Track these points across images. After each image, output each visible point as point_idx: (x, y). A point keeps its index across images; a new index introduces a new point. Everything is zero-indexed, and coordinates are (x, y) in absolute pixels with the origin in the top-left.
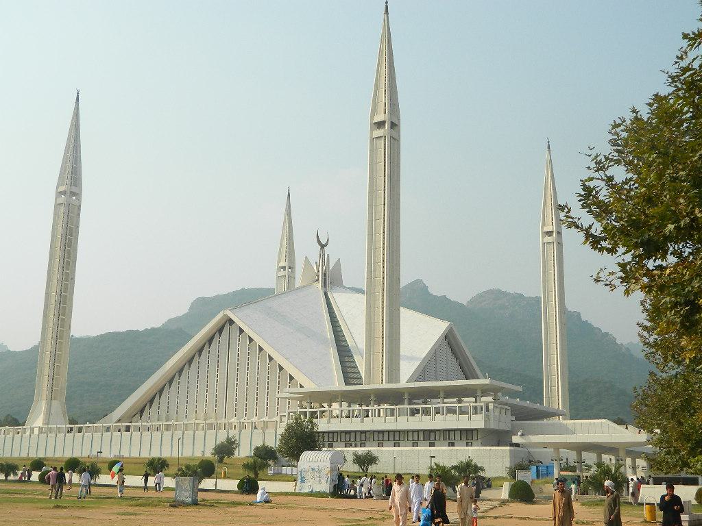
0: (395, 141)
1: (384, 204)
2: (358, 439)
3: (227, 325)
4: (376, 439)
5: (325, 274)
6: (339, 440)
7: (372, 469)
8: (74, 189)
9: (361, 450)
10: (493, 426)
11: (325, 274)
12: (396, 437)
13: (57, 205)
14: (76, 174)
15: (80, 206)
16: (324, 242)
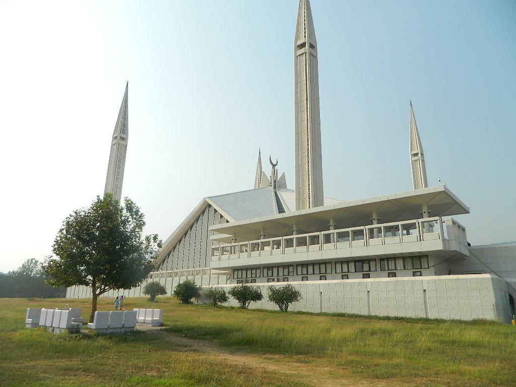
0: (313, 57)
1: (307, 100)
2: (281, 274)
3: (207, 210)
4: (300, 273)
5: (275, 181)
6: (262, 276)
7: (292, 307)
8: (123, 136)
9: (279, 285)
10: (454, 247)
11: (275, 181)
12: (321, 268)
13: (113, 145)
14: (124, 127)
15: (127, 145)
16: (275, 163)
